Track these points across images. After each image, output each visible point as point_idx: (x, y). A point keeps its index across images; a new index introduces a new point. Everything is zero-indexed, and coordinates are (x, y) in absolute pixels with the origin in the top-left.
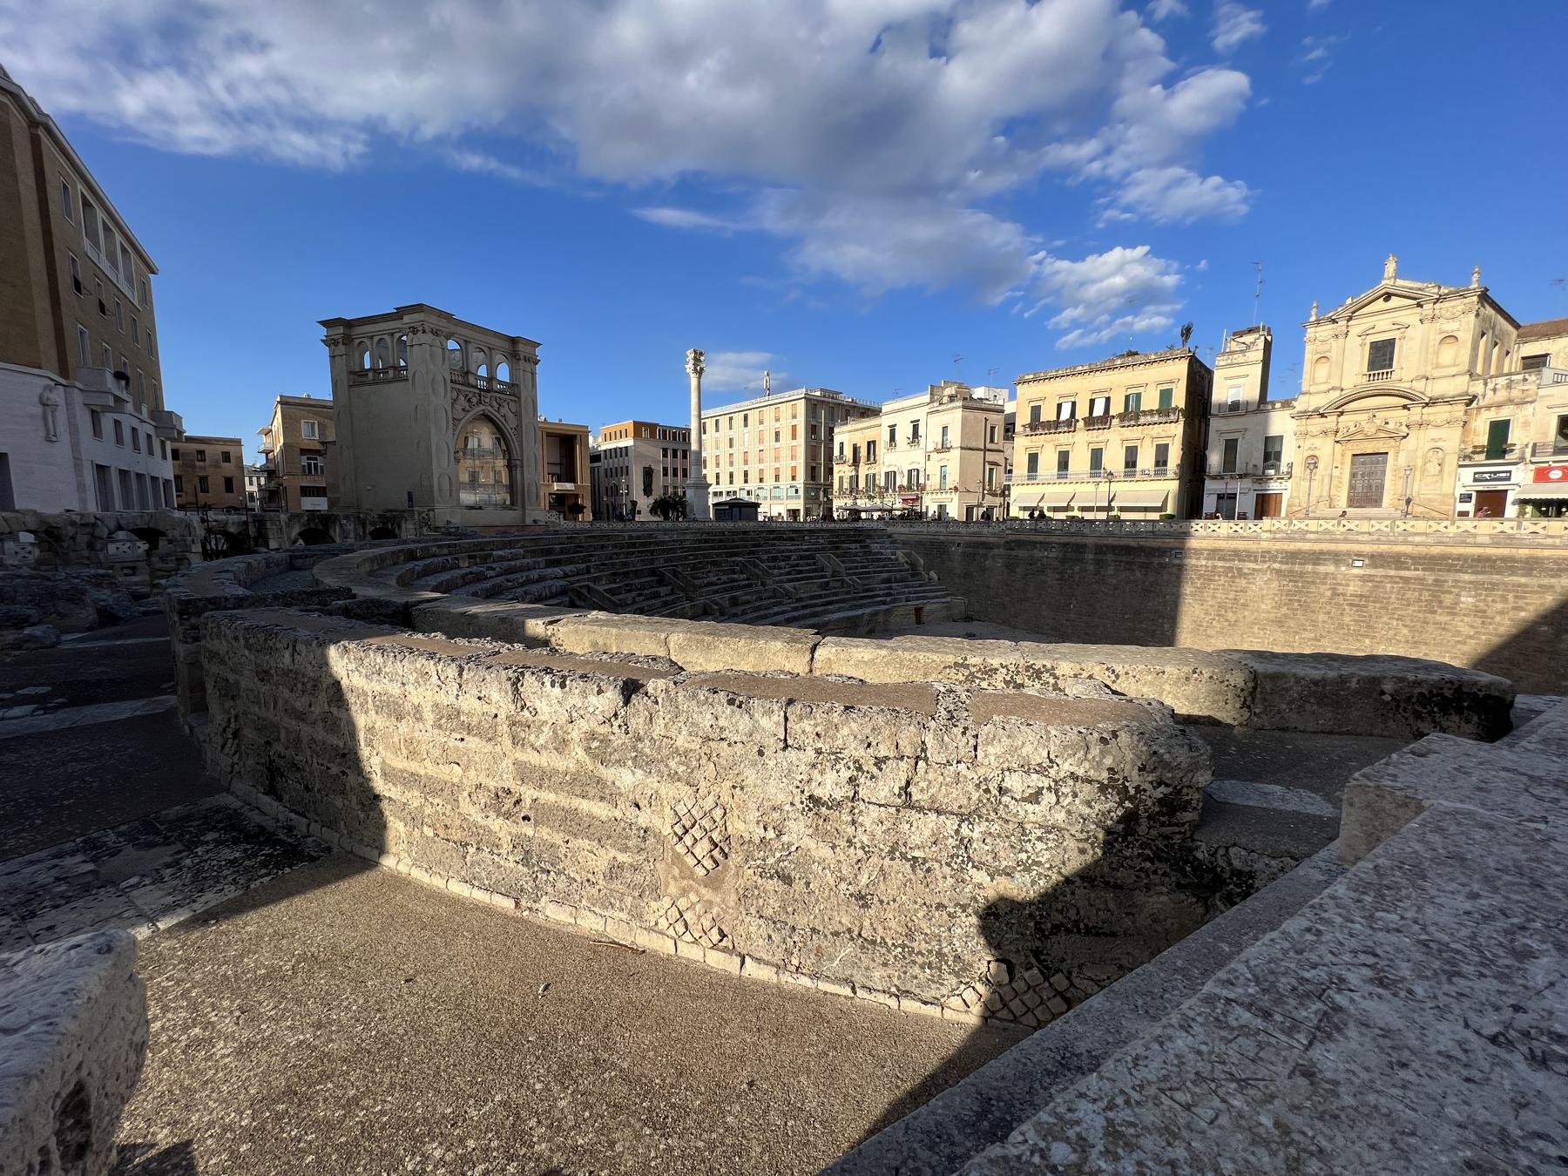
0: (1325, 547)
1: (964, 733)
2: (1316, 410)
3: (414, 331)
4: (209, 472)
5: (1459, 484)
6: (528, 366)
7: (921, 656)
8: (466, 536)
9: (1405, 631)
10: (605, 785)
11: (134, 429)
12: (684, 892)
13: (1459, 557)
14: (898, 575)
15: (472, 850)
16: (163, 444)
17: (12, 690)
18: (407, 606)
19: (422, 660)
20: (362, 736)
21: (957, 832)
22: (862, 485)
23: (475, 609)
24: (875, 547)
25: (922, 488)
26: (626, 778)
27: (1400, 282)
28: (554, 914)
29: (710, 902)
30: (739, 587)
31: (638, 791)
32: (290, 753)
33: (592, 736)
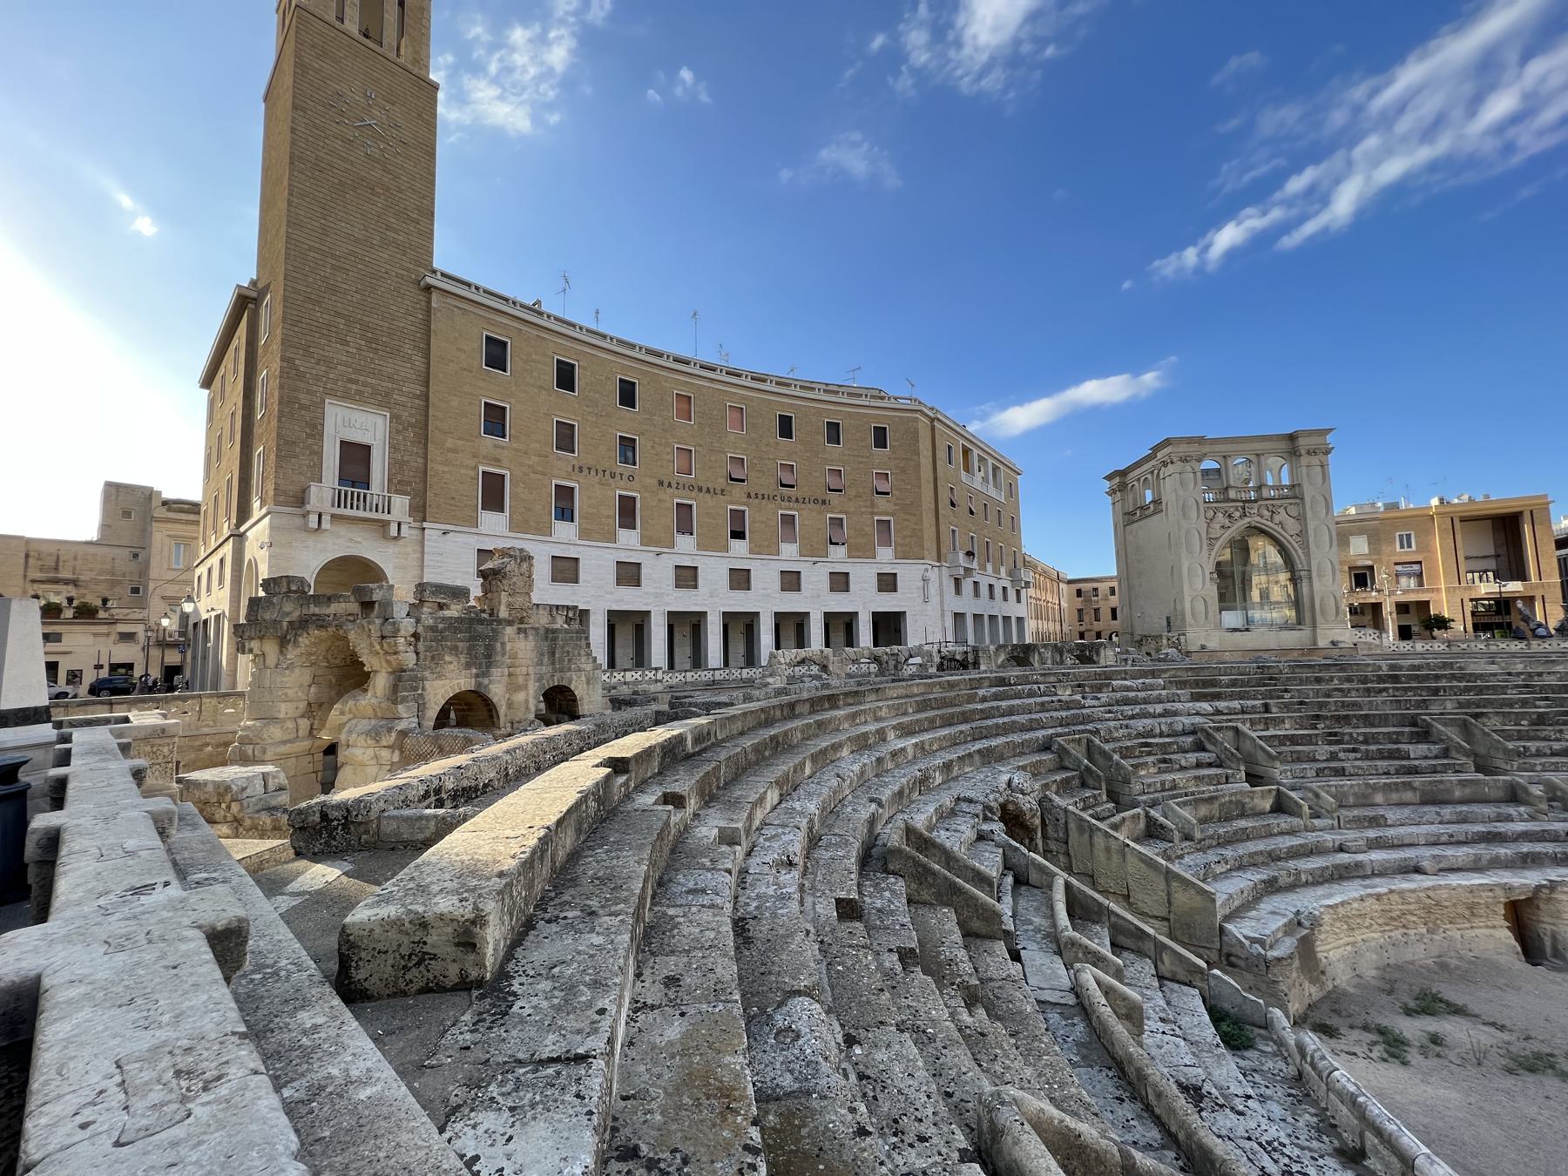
3: (1165, 464)
6: (1315, 460)
11: (991, 586)
16: (1018, 592)
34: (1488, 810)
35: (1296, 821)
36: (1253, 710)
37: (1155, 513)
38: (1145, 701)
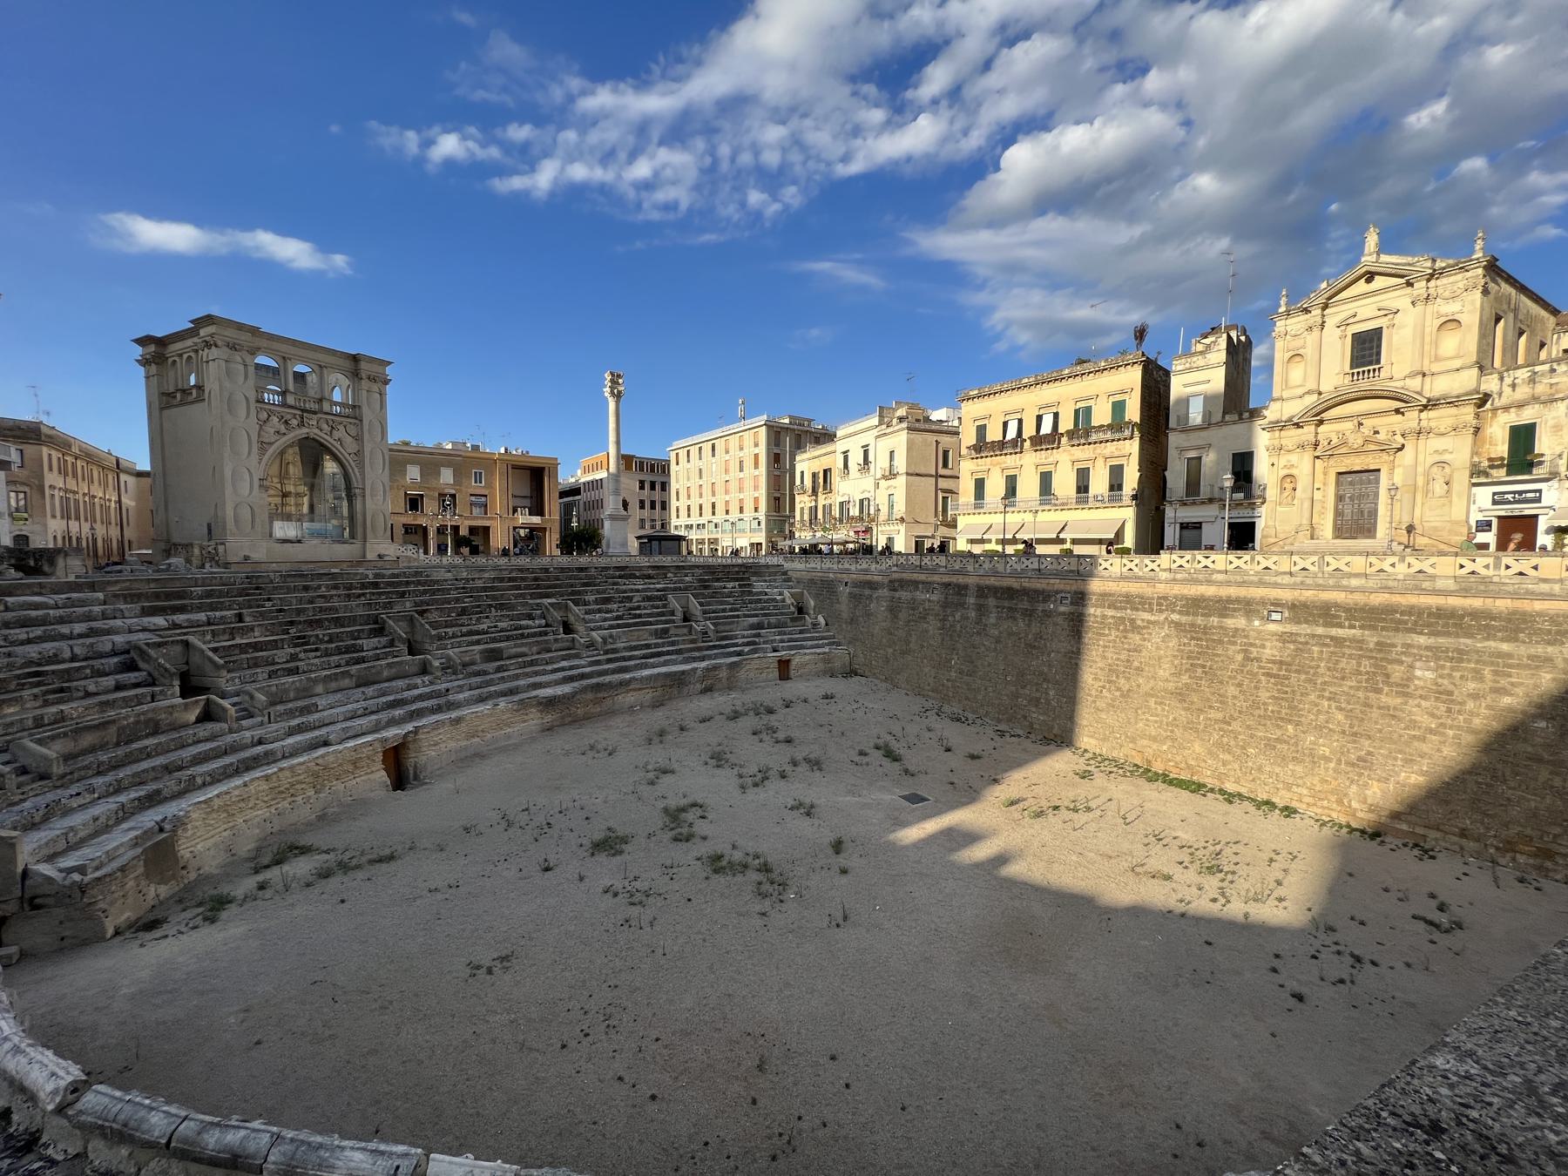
0: (1233, 592)
2: (1290, 420)
3: (208, 345)
5: (1473, 508)
6: (375, 387)
9: (1340, 717)
13: (1410, 610)
14: (773, 620)
22: (820, 516)
24: (759, 586)
27: (1384, 258)
34: (400, 683)
35: (224, 726)
36: (223, 620)
37: (200, 400)
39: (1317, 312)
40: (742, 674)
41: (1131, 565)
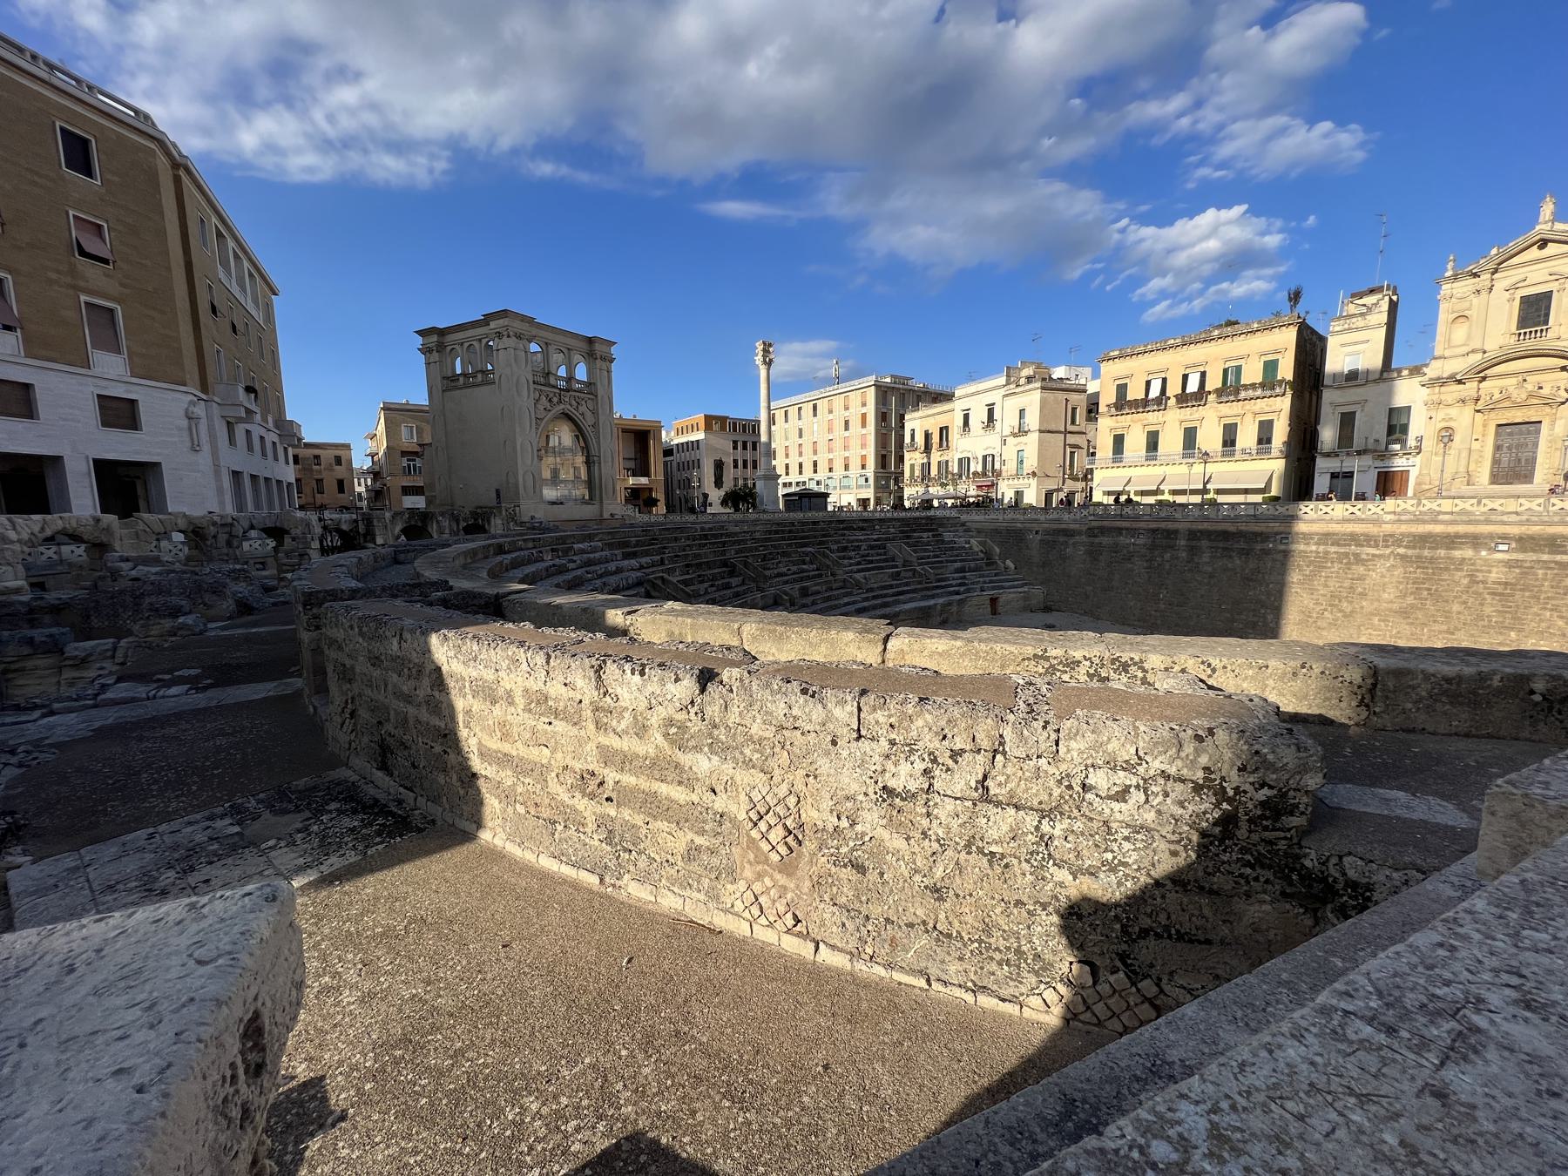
0: (1461, 529)
1: (1044, 727)
3: (499, 335)
4: (324, 475)
6: (604, 365)
7: (997, 647)
8: (549, 530)
9: (1561, 623)
10: (682, 771)
11: (262, 438)
12: (759, 876)
14: (972, 564)
15: (560, 828)
17: (170, 672)
18: (497, 596)
19: (513, 649)
20: (460, 718)
21: (1037, 828)
22: (934, 471)
23: (558, 600)
24: (947, 536)
25: (999, 474)
26: (703, 764)
27: (1559, 226)
28: (636, 891)
29: (785, 888)
30: (809, 578)
31: (715, 776)
32: (398, 732)
33: (670, 722)
37: (487, 383)
38: (599, 562)
39: (1486, 276)
40: (967, 609)
41: (1352, 510)
